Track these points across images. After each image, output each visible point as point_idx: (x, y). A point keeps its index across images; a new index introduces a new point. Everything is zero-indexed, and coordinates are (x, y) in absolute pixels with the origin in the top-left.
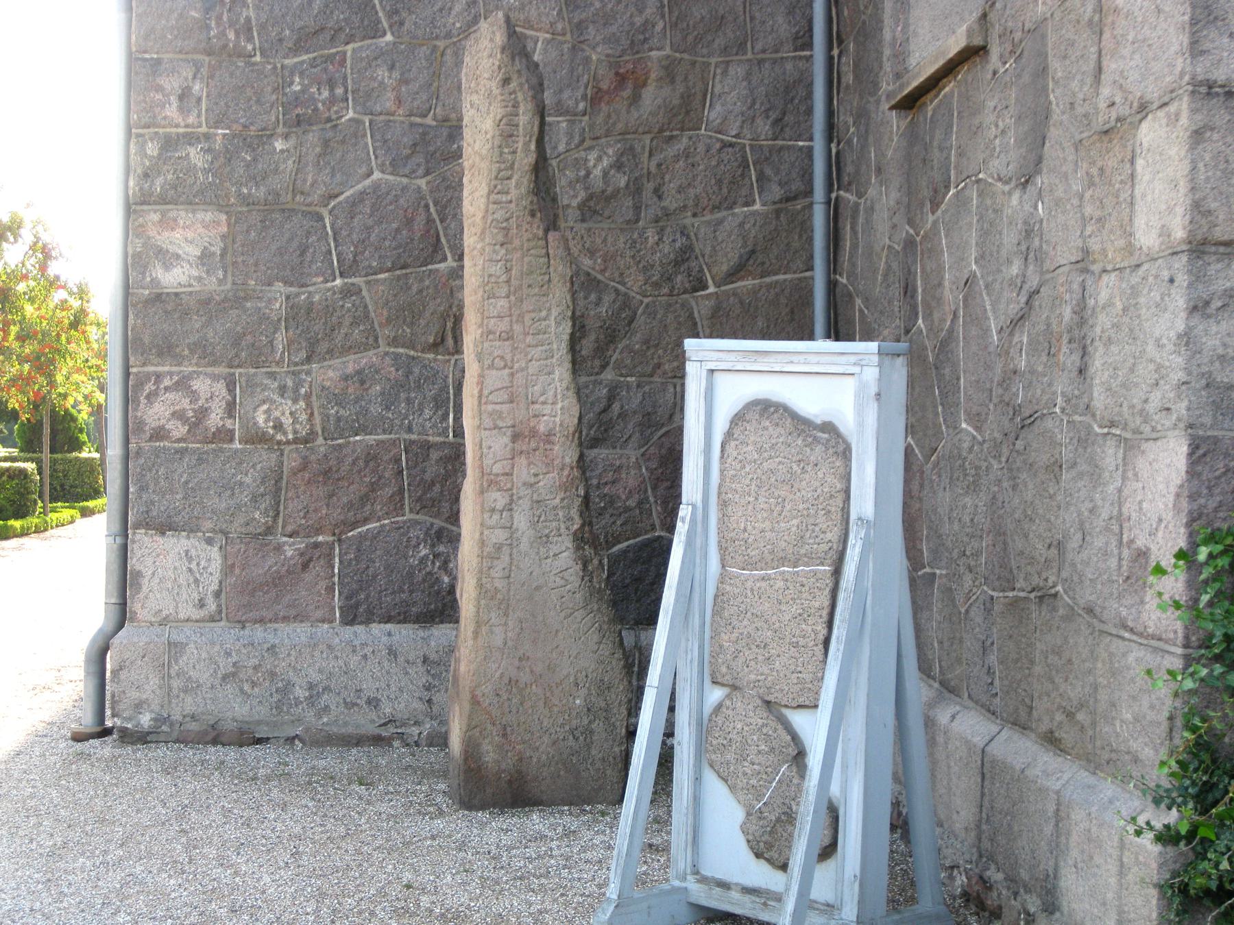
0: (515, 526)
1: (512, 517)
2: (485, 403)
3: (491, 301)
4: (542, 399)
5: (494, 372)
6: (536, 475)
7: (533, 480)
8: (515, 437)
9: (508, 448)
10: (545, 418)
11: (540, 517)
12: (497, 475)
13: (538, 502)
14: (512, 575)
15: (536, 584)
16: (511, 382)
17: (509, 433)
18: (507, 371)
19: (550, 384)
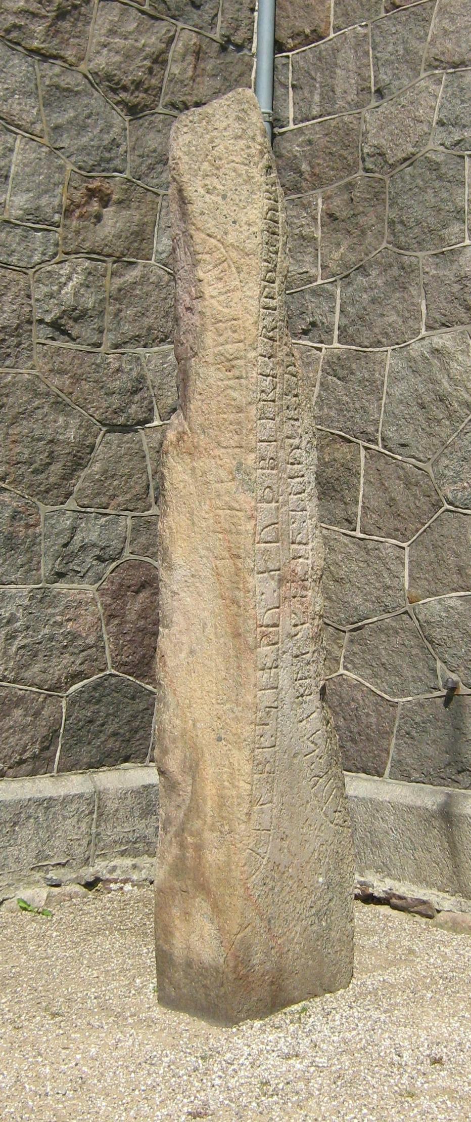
0: (280, 686)
1: (277, 675)
2: (258, 543)
3: (262, 421)
4: (298, 539)
5: (265, 505)
6: (296, 625)
7: (294, 631)
8: (281, 581)
9: (275, 595)
10: (301, 560)
11: (298, 673)
12: (267, 626)
13: (297, 656)
14: (278, 743)
15: (294, 752)
16: (277, 517)
17: (276, 578)
18: (274, 505)
19: (304, 522)
